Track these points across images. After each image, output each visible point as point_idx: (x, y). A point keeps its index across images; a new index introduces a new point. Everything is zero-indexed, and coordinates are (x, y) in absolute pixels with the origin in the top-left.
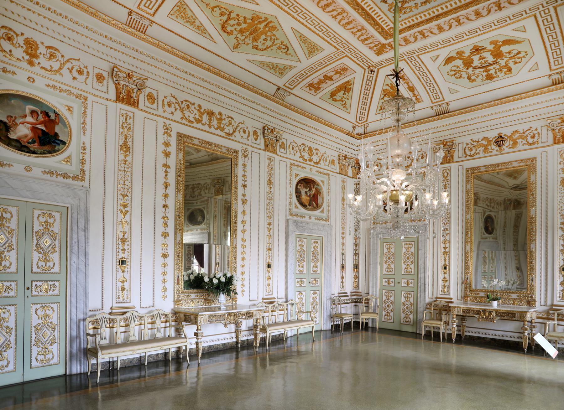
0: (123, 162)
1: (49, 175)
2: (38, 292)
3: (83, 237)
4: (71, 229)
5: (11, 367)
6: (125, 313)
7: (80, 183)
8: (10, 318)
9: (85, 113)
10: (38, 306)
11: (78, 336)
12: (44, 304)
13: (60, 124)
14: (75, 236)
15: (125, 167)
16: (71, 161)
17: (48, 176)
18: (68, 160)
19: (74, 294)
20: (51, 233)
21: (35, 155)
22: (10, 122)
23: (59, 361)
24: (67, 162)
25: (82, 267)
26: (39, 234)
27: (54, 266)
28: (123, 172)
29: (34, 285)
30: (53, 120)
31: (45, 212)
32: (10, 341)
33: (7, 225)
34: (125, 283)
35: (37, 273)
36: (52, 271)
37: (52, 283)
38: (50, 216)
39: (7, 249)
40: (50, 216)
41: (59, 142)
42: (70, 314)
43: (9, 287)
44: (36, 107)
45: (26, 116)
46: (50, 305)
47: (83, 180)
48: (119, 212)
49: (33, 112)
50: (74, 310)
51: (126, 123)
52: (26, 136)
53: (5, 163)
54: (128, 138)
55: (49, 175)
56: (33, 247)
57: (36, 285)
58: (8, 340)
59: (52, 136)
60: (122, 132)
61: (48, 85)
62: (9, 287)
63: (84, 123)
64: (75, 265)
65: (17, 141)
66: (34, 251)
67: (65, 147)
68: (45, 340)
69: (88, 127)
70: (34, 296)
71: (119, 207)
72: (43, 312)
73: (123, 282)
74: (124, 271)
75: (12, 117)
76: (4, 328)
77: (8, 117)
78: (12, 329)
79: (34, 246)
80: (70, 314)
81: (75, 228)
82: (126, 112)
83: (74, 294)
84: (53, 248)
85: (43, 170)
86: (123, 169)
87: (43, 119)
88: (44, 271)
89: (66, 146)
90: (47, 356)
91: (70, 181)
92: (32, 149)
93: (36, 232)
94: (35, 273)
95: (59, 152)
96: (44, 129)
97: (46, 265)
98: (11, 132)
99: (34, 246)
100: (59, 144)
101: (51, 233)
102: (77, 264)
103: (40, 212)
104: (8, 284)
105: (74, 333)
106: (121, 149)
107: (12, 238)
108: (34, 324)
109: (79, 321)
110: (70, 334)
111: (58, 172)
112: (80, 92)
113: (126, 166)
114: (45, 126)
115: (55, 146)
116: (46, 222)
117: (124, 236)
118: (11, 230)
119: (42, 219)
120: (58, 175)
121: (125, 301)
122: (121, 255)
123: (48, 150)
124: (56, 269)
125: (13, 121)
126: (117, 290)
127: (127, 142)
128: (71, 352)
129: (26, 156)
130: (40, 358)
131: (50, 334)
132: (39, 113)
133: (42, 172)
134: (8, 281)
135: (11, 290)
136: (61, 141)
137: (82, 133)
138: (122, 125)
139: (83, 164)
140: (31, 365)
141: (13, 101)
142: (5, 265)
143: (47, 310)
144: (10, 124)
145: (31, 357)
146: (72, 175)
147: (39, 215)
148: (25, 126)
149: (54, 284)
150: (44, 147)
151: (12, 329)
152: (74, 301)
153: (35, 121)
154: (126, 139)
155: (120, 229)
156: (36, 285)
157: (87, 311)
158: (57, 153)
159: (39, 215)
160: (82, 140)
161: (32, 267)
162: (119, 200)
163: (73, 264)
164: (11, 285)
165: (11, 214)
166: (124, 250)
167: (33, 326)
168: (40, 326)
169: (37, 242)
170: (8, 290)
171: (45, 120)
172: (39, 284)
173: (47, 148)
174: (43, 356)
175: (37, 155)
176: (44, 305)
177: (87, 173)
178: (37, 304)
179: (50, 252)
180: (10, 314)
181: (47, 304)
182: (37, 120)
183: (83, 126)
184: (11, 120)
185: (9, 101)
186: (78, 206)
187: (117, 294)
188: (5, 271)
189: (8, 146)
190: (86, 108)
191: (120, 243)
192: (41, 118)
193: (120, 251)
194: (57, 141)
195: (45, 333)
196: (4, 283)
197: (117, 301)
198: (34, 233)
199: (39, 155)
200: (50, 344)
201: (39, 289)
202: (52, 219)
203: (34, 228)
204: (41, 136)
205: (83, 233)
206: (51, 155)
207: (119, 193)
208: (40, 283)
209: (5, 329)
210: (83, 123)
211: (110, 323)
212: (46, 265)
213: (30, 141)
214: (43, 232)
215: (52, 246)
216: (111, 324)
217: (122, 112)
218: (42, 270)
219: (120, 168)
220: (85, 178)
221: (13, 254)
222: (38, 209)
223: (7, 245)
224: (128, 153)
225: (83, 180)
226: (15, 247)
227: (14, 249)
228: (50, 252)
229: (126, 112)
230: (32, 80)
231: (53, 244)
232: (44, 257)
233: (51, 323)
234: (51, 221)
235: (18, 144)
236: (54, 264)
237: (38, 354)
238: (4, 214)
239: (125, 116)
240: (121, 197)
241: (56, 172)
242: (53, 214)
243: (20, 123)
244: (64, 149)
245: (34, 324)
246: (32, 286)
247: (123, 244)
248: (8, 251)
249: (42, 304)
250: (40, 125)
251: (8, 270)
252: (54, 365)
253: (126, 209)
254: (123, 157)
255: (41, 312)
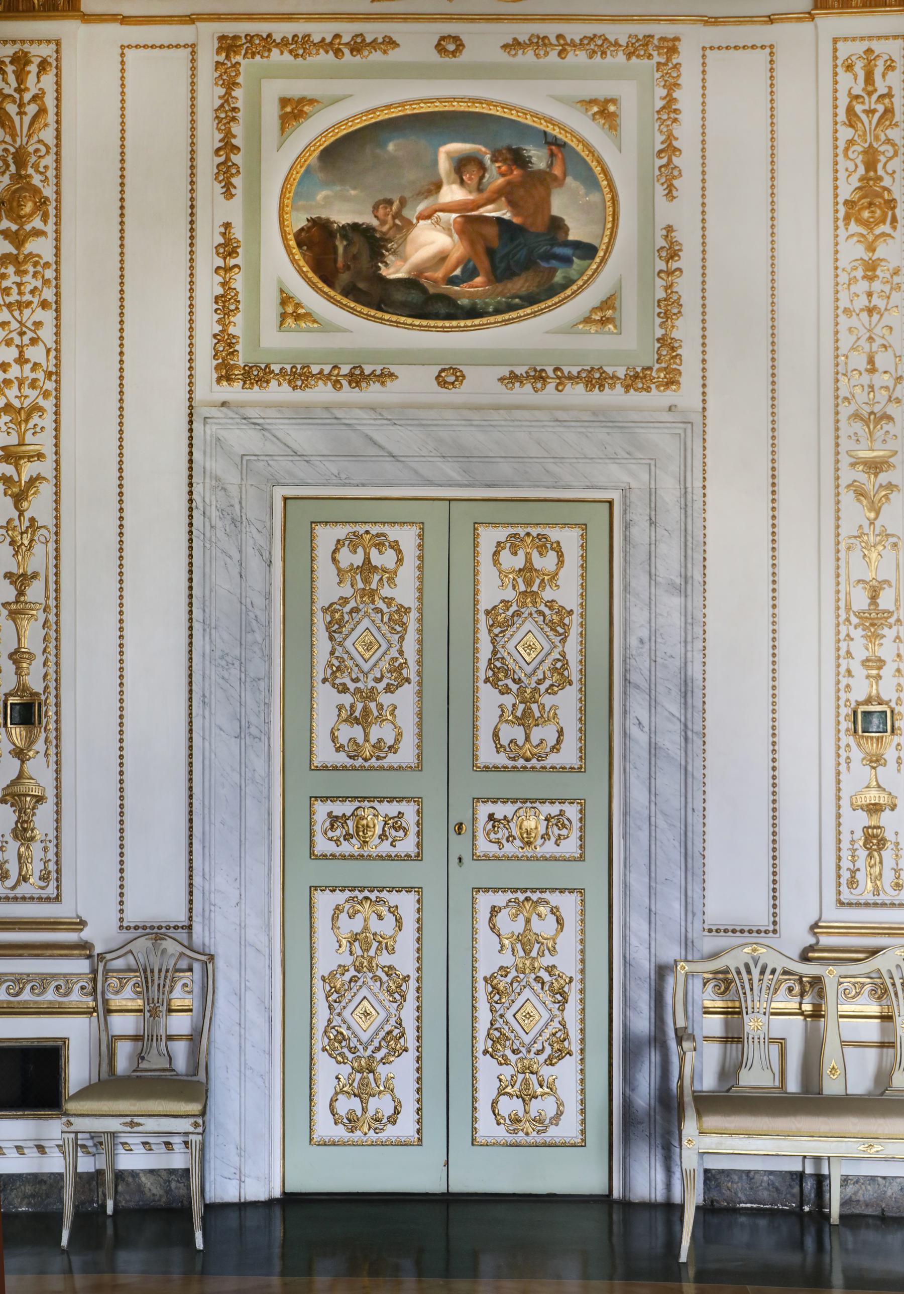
0: (860, 273)
1: (528, 387)
2: (498, 842)
3: (677, 620)
4: (626, 588)
5: (406, 1127)
6: (873, 952)
7: (657, 398)
8: (400, 936)
9: (670, 104)
10: (500, 899)
11: (658, 1039)
12: (523, 890)
13: (569, 180)
14: (639, 616)
15: (870, 295)
16: (616, 315)
17: (524, 393)
18: (609, 313)
19: (639, 857)
20: (547, 611)
21: (477, 321)
22: (383, 222)
23: (583, 1132)
24: (604, 321)
25: (670, 741)
26: (500, 619)
27: (559, 741)
28: (864, 316)
29: (482, 817)
30: (540, 172)
31: (521, 531)
32: (399, 1023)
33: (386, 591)
34: (886, 815)
35: (496, 768)
36: (553, 760)
37: (554, 810)
38: (543, 544)
39: (385, 681)
40: (543, 544)
41: (567, 251)
42: (625, 939)
43: (396, 823)
44: (474, 142)
45: (438, 186)
46: (547, 896)
47: (671, 381)
48: (847, 497)
49: (461, 165)
50: (639, 925)
51: (870, 94)
52: (442, 258)
53: (367, 372)
54: (883, 159)
55: (528, 387)
56: (475, 669)
57: (491, 817)
58: (392, 1021)
59: (538, 235)
60: (851, 142)
61: (514, 45)
62: (396, 823)
63: (670, 149)
64: (640, 737)
65: (411, 283)
66: (481, 684)
67: (594, 266)
68: (527, 1039)
69: (687, 161)
70: (487, 858)
71: (848, 475)
72: (519, 926)
73: (874, 809)
74: (875, 761)
75: (389, 202)
76: (379, 973)
77: (375, 208)
78: (406, 979)
79: (483, 664)
80: (625, 939)
81: (640, 582)
82: (865, 45)
83: (639, 857)
84: (554, 670)
85: (505, 371)
86: (863, 301)
87: (501, 181)
88: (521, 762)
89: (597, 260)
90: (535, 1106)
91: (614, 396)
92: (464, 302)
93: (487, 613)
94: (487, 768)
95: (568, 292)
96: (507, 216)
97: (527, 738)
98: (390, 258)
99: (483, 664)
100: (567, 261)
101: (547, 611)
102: (653, 732)
103: (502, 534)
104: (392, 809)
105: (642, 1024)
106: (847, 218)
107: (401, 639)
108: (485, 969)
109: (662, 972)
110: (625, 1026)
111: (566, 370)
112: (641, 30)
113: (877, 286)
114: (513, 204)
115: (553, 271)
116: (528, 570)
117: (874, 598)
118: (398, 611)
119: (512, 561)
120: (563, 379)
121: (887, 899)
122: (860, 689)
123: (523, 292)
124: (568, 755)
125: (394, 218)
126: (845, 845)
127: (880, 179)
128: (627, 1105)
129: (444, 329)
130: (509, 1106)
131: (546, 1016)
132: (487, 158)
133: (501, 380)
134: (391, 800)
135: (401, 833)
136: (578, 245)
137: (660, 190)
138: (850, 110)
139: (667, 316)
140: (474, 1130)
141: (391, 147)
142: (380, 740)
143: (534, 918)
144: (385, 228)
145: (474, 1099)
146: (621, 372)
147: (499, 543)
148: (438, 222)
149: (562, 813)
150: (509, 285)
151: (406, 979)
152: (638, 884)
153: (471, 197)
154: (871, 165)
155: (857, 568)
156: (491, 817)
157: (696, 930)
158: (562, 295)
159: (499, 543)
160: (661, 222)
161: (474, 747)
162: (846, 444)
163: (634, 731)
164: (400, 815)
165: (399, 552)
166: (880, 663)
167: (480, 976)
168: (509, 979)
169: (495, 652)
170: (394, 833)
171: (509, 183)
172: (501, 810)
173: (520, 285)
174: (518, 1104)
175: (484, 320)
176: (521, 897)
177: (689, 354)
178: (496, 890)
179: (543, 688)
180: (399, 921)
181: (533, 890)
182: (480, 189)
183: (664, 161)
184: (387, 215)
185: (378, 151)
186: (652, 493)
187: (846, 864)
188: (380, 763)
189: (379, 309)
190: (672, 86)
191: (857, 633)
192: (495, 178)
193: (860, 672)
194: (559, 250)
195: (529, 1008)
196: (376, 804)
197: (846, 896)
198: (482, 617)
199: (492, 319)
200: (545, 1056)
201: (502, 834)
202: (552, 555)
203: (482, 597)
204: (495, 243)
205: (676, 601)
206: (535, 308)
207: (846, 410)
208: (507, 810)
209: (385, 978)
210: (661, 151)
211: (802, 995)
212: (527, 738)
213: (458, 272)
214: (514, 608)
215: (549, 661)
216: (807, 999)
217: (845, 49)
218: (514, 759)
219: (844, 303)
220: (680, 373)
221: (405, 697)
222: (495, 524)
223: (384, 665)
224: (886, 228)
225: (671, 381)
226: (411, 672)
227: (408, 680)
228: (543, 688)
229: (863, 46)
230: (451, 47)
231: (555, 655)
232: (521, 707)
233: (550, 970)
234: (545, 563)
235: (414, 296)
236: (561, 732)
237: (501, 1092)
238: (374, 552)
239: (859, 68)
240: (858, 426)
241: (556, 369)
242: (554, 534)
243: (418, 219)
244: (590, 272)
245: (485, 969)
246: (474, 819)
247: (874, 637)
248: (389, 689)
249: (515, 890)
250: (490, 207)
251: (392, 759)
252: (556, 1146)
253: (883, 478)
254: (860, 251)
255: (509, 924)
